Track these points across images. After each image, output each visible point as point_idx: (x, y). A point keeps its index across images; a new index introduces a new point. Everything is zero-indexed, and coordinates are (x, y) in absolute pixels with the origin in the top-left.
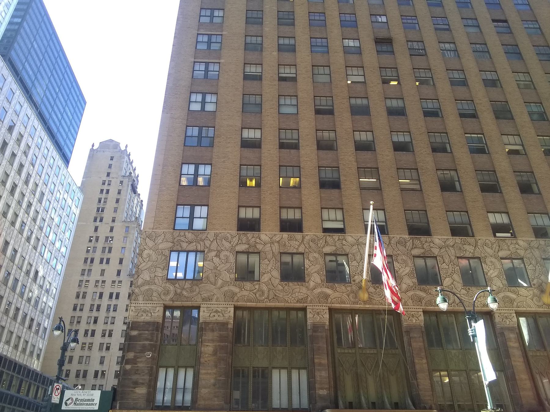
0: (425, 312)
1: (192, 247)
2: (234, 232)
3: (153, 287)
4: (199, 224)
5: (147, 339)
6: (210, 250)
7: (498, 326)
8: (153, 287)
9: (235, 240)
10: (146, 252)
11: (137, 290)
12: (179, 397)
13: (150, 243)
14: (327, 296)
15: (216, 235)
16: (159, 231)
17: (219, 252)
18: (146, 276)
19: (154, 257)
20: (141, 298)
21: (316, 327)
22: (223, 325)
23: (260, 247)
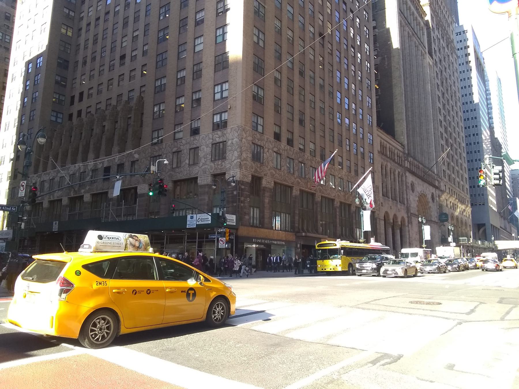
0: (322, 197)
1: (259, 144)
2: (273, 139)
3: (247, 162)
4: (260, 128)
5: (247, 191)
6: (266, 148)
7: (335, 206)
8: (247, 162)
9: (273, 144)
10: (243, 140)
11: (242, 163)
12: (255, 221)
13: (245, 135)
14: (299, 183)
15: (267, 139)
16: (248, 128)
17: (269, 149)
18: (244, 155)
19: (246, 144)
20: (243, 167)
21: (296, 197)
22: (270, 189)
23: (281, 151)
